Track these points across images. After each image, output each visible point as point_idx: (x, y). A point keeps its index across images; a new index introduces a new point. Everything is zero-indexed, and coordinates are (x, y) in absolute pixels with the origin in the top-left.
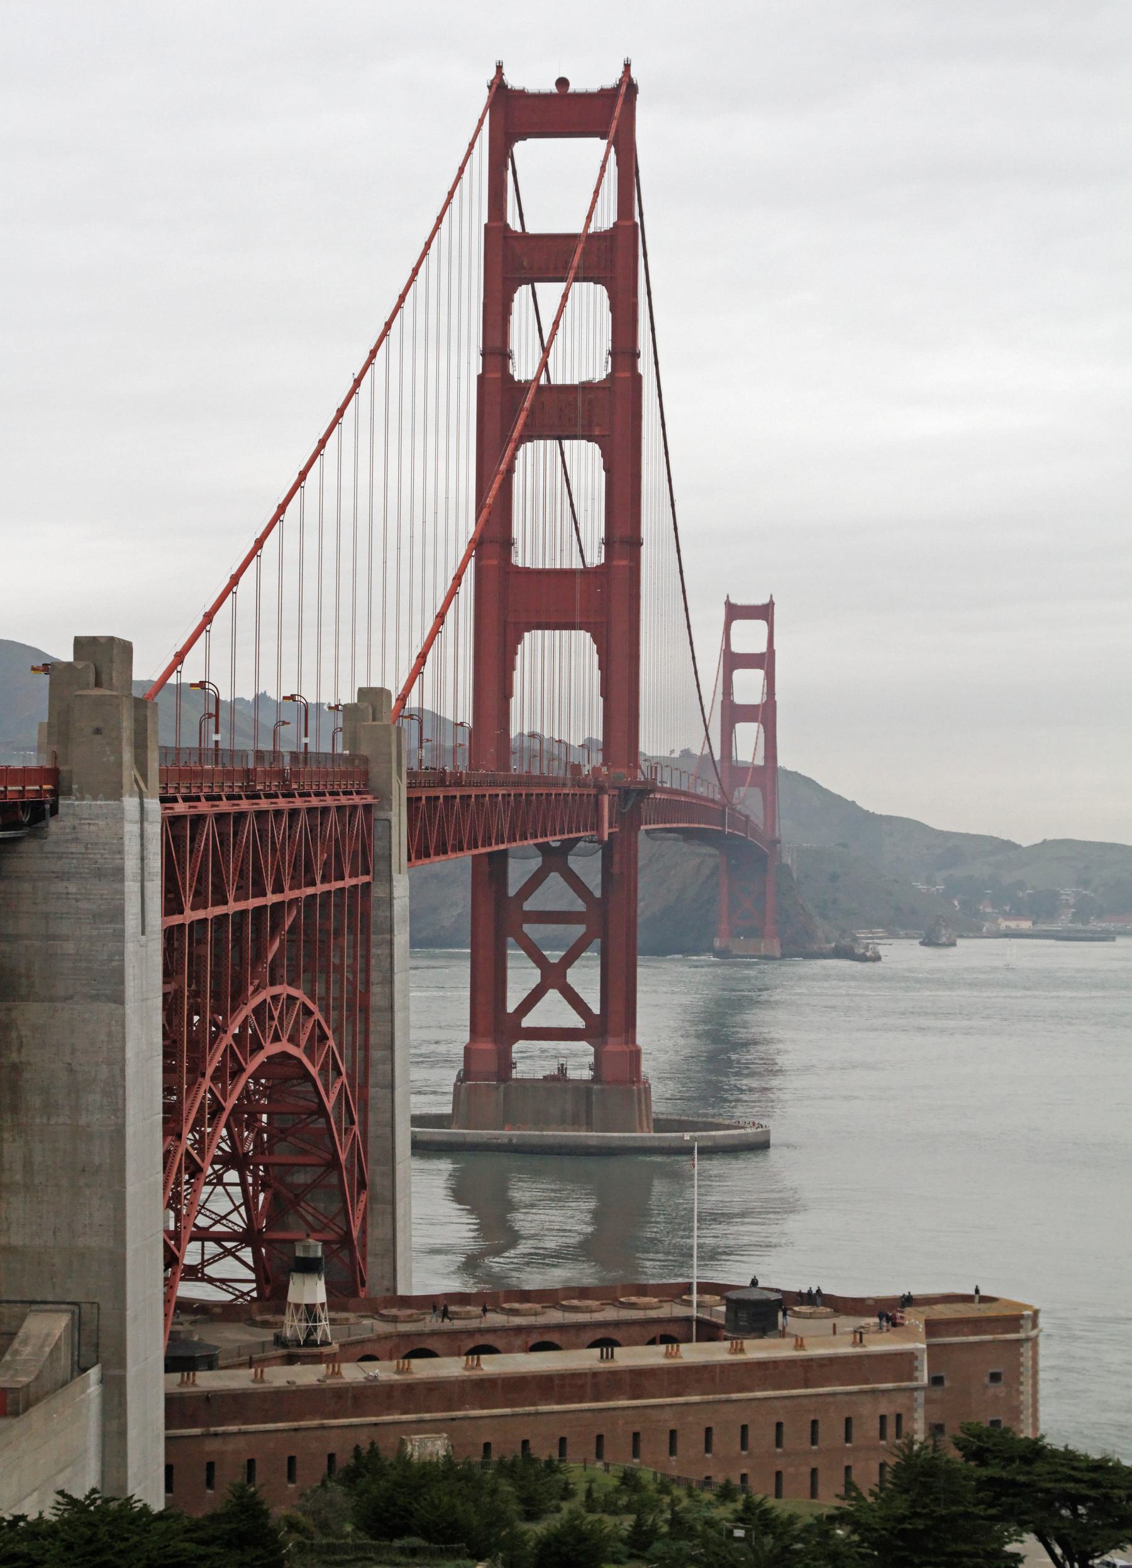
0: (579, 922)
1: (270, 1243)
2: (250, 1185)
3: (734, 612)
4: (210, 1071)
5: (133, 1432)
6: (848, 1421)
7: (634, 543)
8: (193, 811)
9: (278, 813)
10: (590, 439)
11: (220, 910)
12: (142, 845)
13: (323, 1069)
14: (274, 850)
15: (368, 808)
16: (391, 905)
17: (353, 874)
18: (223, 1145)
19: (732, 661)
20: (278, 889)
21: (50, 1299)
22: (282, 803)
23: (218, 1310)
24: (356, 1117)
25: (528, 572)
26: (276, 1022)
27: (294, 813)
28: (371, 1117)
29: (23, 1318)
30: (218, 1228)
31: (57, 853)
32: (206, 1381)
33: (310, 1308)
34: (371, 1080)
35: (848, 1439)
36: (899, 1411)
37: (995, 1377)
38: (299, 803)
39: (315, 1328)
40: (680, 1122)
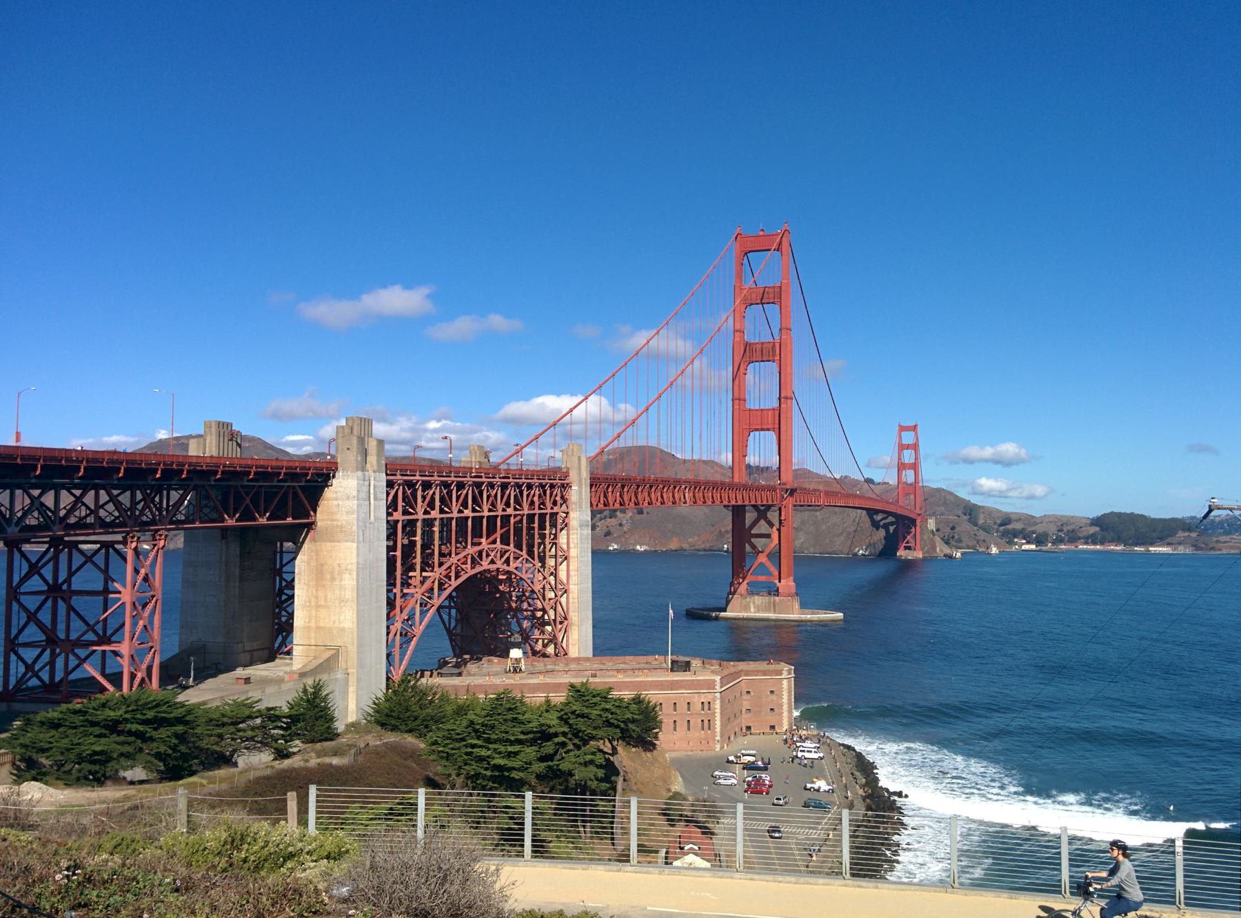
19: (902, 447)
28: (570, 595)
34: (571, 582)
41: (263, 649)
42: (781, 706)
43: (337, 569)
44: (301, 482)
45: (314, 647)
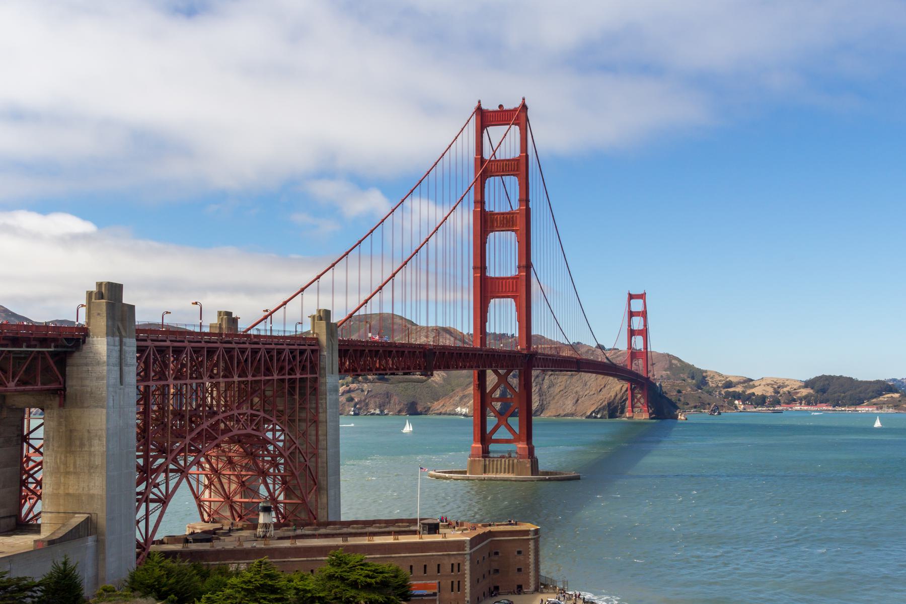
3: (631, 297)
6: (439, 565)
8: (173, 345)
9: (243, 351)
10: (513, 231)
19: (631, 314)
21: (81, 512)
25: (491, 278)
28: (319, 460)
35: (439, 572)
36: (459, 562)
37: (519, 552)
40: (551, 472)
41: (10, 517)
42: (528, 565)
43: (86, 434)
44: (51, 348)
45: (62, 515)
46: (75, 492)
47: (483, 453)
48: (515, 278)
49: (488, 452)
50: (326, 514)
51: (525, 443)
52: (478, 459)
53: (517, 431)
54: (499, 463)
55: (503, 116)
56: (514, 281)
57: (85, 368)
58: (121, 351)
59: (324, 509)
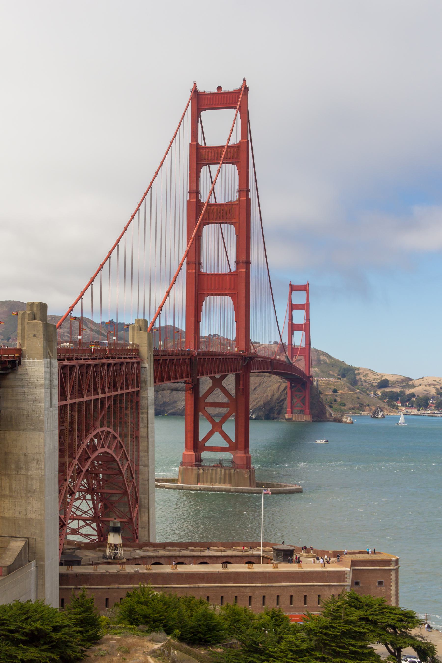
0: (227, 407)
1: (103, 522)
2: (95, 500)
4: (77, 457)
5: (47, 585)
7: (248, 263)
9: (103, 365)
10: (231, 223)
11: (81, 400)
12: (51, 376)
13: (121, 459)
14: (102, 378)
15: (138, 363)
16: (147, 399)
17: (133, 388)
18: (86, 485)
19: (292, 307)
20: (103, 392)
21: (19, 536)
22: (104, 361)
23: (83, 545)
24: (134, 476)
26: (102, 440)
27: (109, 365)
28: (140, 477)
29: (9, 542)
30: (83, 516)
31: (21, 378)
32: (77, 569)
33: (116, 545)
34: (140, 463)
38: (110, 361)
39: (118, 553)
43: (23, 457)
46: (10, 516)
47: (196, 461)
48: (231, 274)
49: (201, 461)
50: (147, 533)
51: (243, 452)
52: (191, 467)
53: (233, 438)
54: (214, 472)
55: (221, 98)
56: (233, 277)
57: (21, 390)
58: (50, 373)
59: (145, 528)
